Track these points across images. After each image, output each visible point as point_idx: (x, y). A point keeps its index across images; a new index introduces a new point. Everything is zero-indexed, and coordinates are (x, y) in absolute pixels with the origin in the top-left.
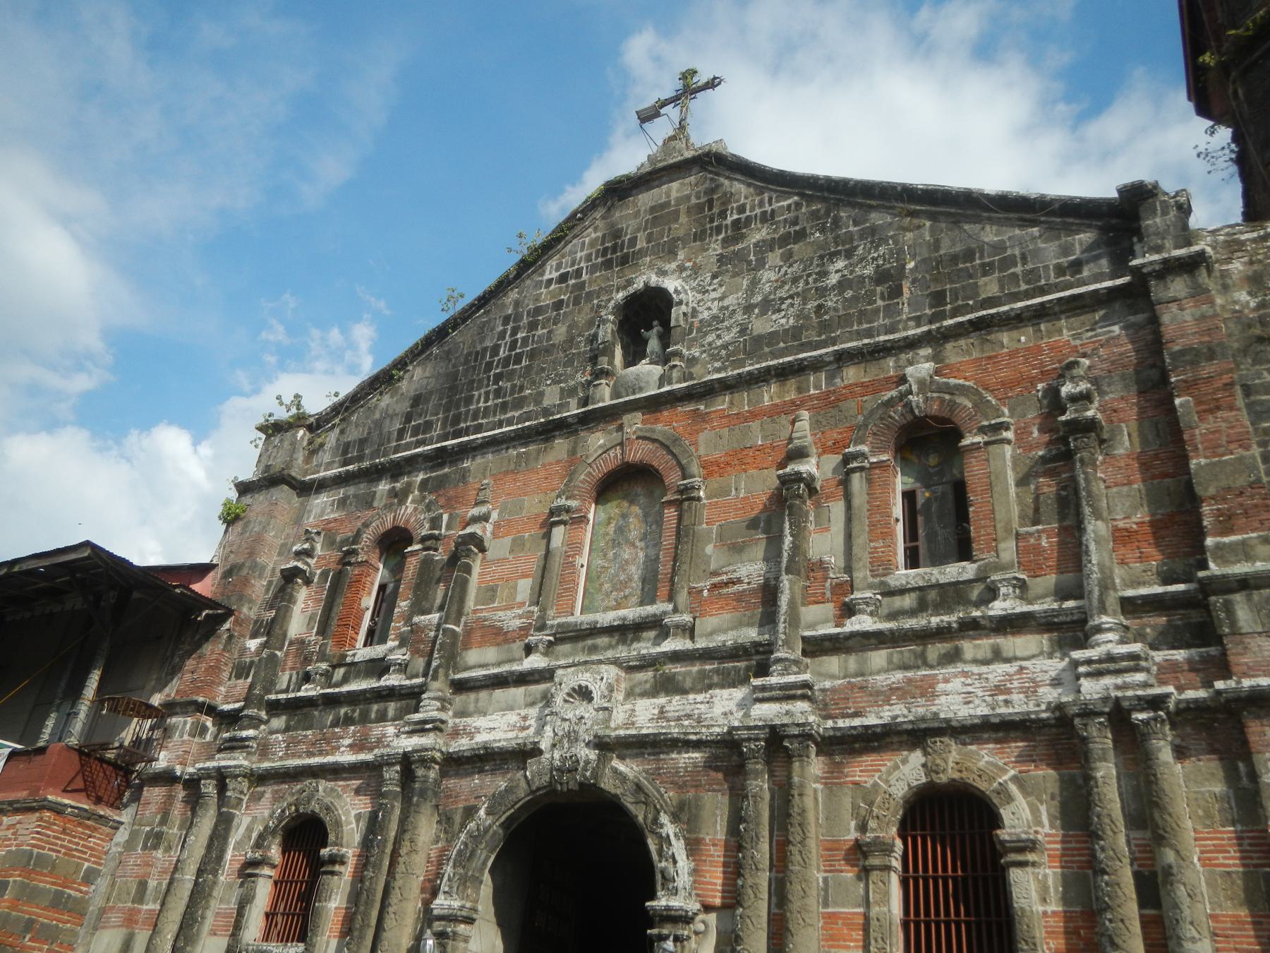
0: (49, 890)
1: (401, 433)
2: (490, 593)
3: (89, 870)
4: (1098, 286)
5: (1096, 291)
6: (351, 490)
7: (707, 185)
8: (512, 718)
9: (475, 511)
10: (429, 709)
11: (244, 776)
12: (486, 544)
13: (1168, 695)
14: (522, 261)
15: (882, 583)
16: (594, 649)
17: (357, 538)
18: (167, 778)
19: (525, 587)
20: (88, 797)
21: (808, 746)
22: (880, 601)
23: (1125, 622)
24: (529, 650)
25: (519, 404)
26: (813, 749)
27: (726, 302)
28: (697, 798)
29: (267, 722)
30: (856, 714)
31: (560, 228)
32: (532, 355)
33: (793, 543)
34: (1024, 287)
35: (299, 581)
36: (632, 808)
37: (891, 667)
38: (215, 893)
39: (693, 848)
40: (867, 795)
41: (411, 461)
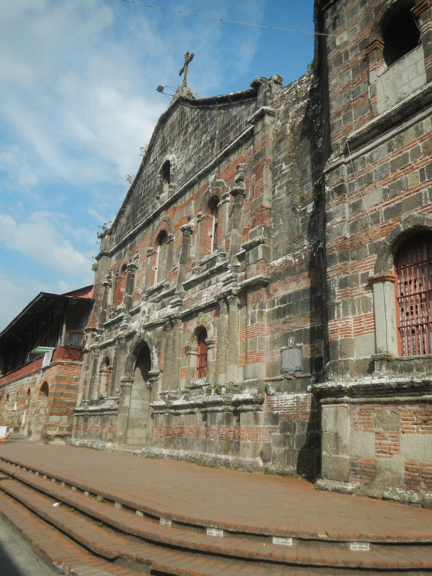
0: (65, 385)
3: (76, 378)
4: (248, 130)
5: (248, 132)
9: (136, 255)
10: (124, 323)
11: (98, 348)
12: (137, 266)
13: (231, 290)
14: (144, 158)
15: (200, 262)
18: (86, 351)
20: (71, 359)
21: (176, 321)
22: (200, 268)
23: (239, 264)
26: (180, 321)
28: (161, 340)
29: (105, 331)
31: (151, 142)
32: (148, 194)
33: (182, 253)
34: (238, 133)
35: (108, 287)
36: (149, 345)
38: (95, 381)
41: (126, 240)
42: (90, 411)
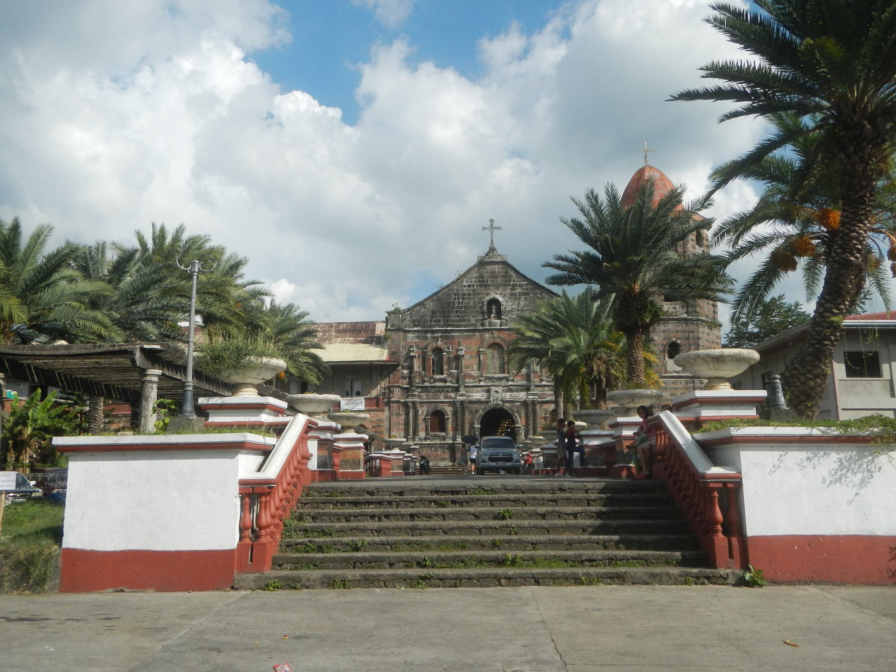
1: (431, 321)
2: (467, 367)
6: (420, 334)
7: (504, 270)
8: (481, 394)
16: (493, 382)
17: (426, 348)
18: (398, 402)
19: (475, 367)
24: (480, 381)
25: (464, 321)
27: (513, 307)
30: (544, 398)
32: (465, 307)
37: (548, 390)
39: (520, 417)
40: (546, 410)
42: (422, 444)
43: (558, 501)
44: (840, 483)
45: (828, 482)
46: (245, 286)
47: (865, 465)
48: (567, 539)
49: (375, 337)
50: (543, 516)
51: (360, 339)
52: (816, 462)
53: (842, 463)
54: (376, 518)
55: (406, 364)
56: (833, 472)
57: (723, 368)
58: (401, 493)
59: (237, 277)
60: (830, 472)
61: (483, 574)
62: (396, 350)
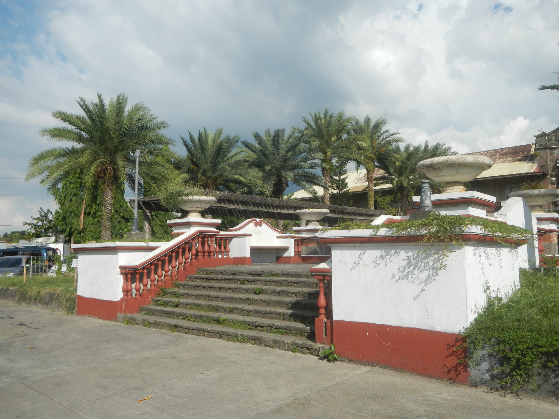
43: (299, 284)
44: (407, 279)
45: (397, 278)
46: (388, 137)
47: (431, 263)
48: (263, 310)
49: (529, 156)
50: (279, 293)
51: (517, 158)
52: (388, 261)
53: (410, 261)
54: (206, 289)
55: (555, 173)
56: (401, 269)
57: (441, 174)
58: (234, 274)
59: (384, 133)
60: (399, 269)
61: (198, 328)
62: (544, 164)
